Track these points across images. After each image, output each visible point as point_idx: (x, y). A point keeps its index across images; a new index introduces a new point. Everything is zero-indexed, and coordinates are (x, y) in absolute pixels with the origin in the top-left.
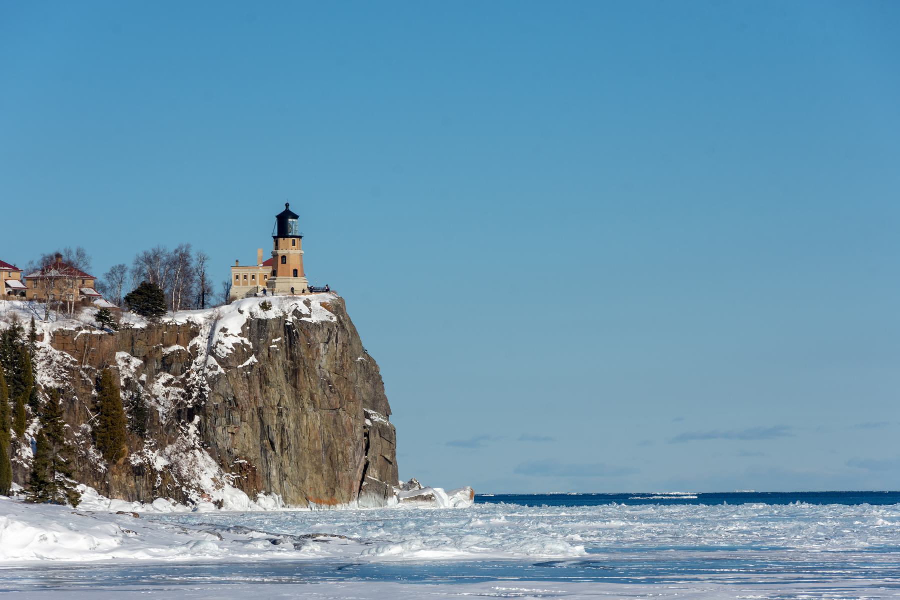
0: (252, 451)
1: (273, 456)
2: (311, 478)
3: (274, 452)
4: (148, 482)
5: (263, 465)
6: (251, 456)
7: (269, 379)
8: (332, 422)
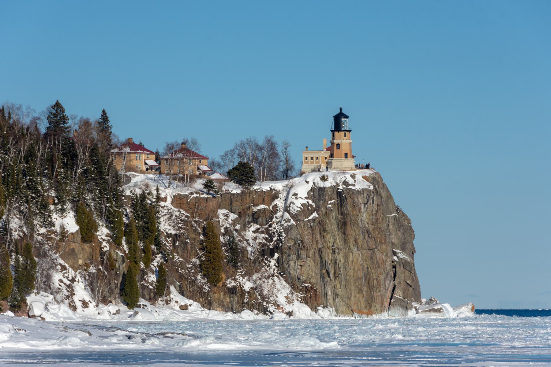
0: (314, 278)
1: (329, 281)
2: (355, 296)
3: (329, 279)
4: (239, 299)
5: (321, 287)
6: (314, 281)
7: (326, 228)
8: (369, 257)
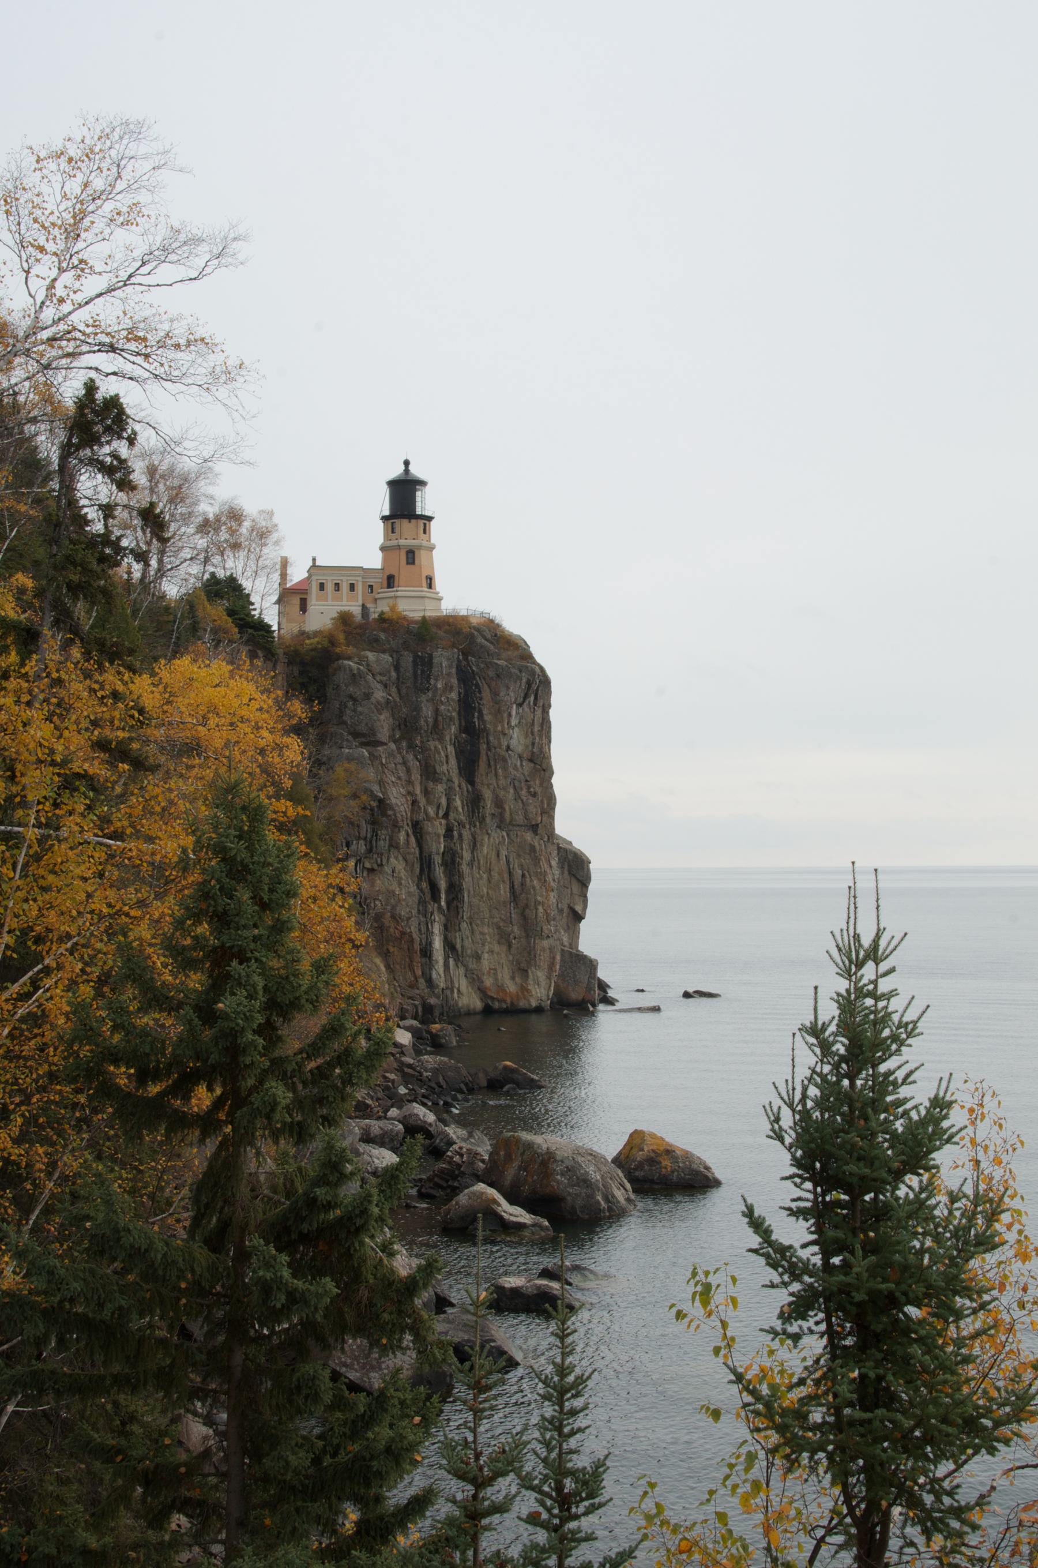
5: (420, 930)
7: (434, 767)
